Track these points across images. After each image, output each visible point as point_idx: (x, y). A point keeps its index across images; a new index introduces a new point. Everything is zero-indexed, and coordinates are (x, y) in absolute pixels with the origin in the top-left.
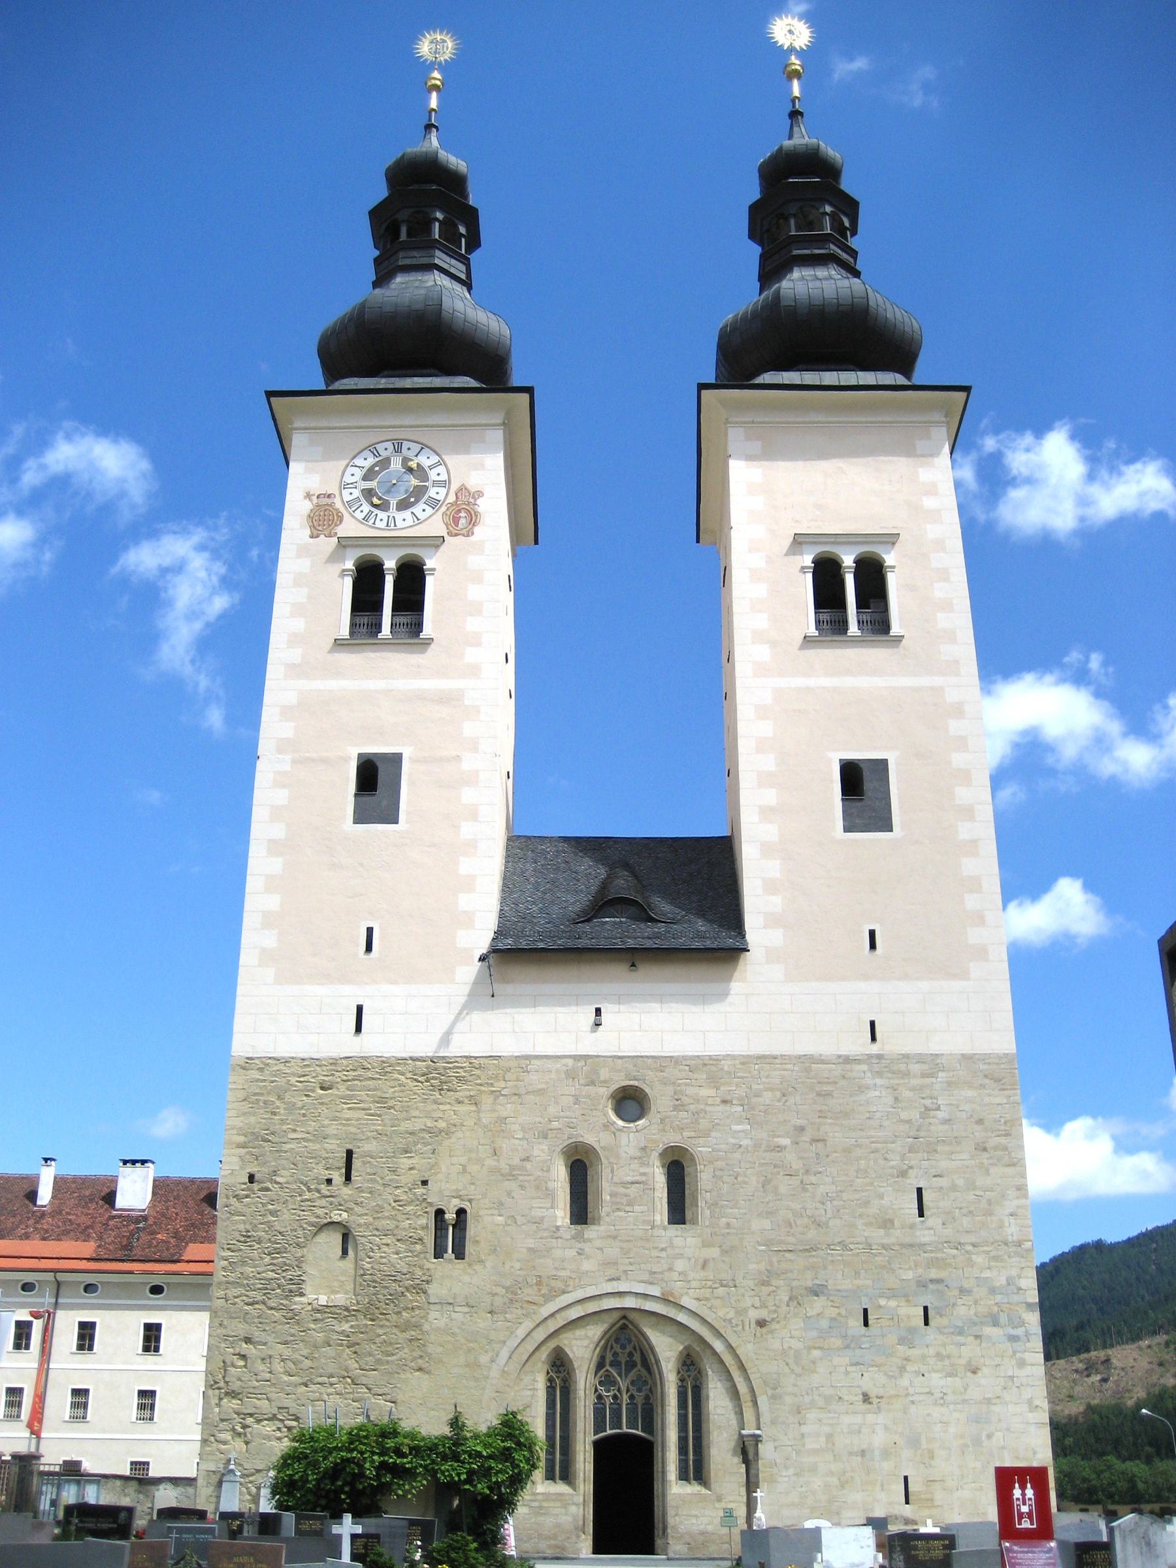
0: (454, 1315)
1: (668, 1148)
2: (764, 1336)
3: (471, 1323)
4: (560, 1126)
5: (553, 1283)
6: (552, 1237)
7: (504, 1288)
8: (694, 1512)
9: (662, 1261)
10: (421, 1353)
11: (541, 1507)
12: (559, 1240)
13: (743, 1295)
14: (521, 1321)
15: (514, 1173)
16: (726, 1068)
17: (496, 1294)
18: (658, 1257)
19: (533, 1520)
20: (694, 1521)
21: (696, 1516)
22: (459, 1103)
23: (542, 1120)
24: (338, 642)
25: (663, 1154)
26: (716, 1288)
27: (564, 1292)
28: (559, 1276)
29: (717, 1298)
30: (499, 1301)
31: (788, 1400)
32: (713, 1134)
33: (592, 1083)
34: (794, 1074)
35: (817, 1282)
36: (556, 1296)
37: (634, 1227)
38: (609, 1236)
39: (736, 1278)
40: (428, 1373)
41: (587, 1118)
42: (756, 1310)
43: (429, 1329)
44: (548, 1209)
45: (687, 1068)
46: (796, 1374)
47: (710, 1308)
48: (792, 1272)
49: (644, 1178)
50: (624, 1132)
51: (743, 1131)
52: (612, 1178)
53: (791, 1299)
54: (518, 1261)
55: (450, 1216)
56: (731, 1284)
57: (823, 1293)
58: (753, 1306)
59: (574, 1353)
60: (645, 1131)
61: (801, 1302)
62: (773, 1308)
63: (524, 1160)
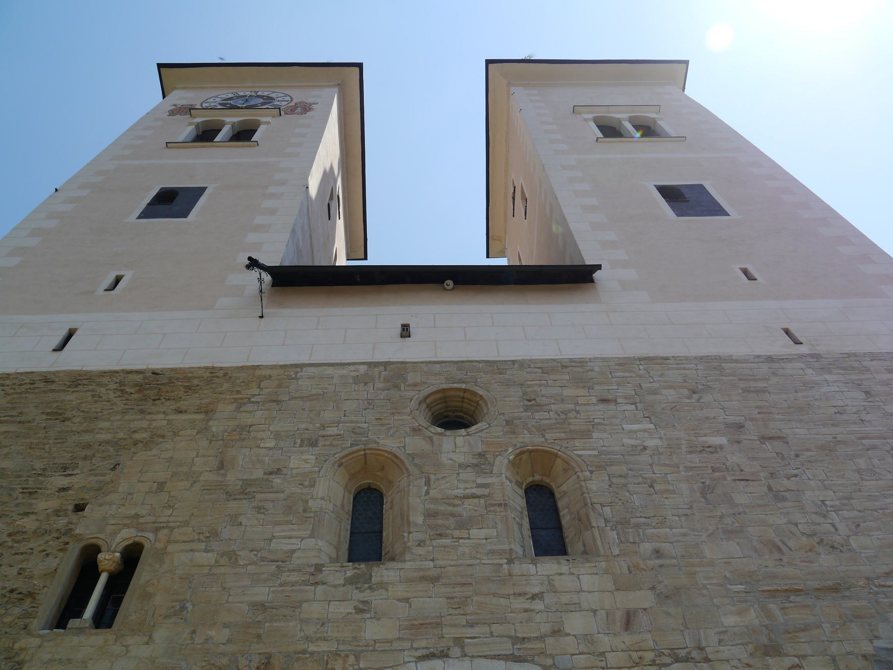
1: (522, 453)
4: (342, 432)
6: (305, 583)
9: (538, 618)
12: (320, 587)
15: (247, 491)
16: (597, 369)
18: (526, 611)
22: (181, 412)
23: (311, 426)
24: (168, 145)
25: (514, 464)
28: (312, 653)
32: (595, 435)
33: (397, 387)
34: (700, 372)
35: (878, 643)
37: (469, 562)
38: (423, 578)
39: (704, 644)
41: (386, 422)
44: (303, 539)
45: (540, 370)
49: (486, 491)
50: (446, 435)
51: (645, 431)
52: (427, 493)
54: (226, 626)
55: (109, 560)
56: (695, 654)
60: (483, 434)
63: (271, 473)
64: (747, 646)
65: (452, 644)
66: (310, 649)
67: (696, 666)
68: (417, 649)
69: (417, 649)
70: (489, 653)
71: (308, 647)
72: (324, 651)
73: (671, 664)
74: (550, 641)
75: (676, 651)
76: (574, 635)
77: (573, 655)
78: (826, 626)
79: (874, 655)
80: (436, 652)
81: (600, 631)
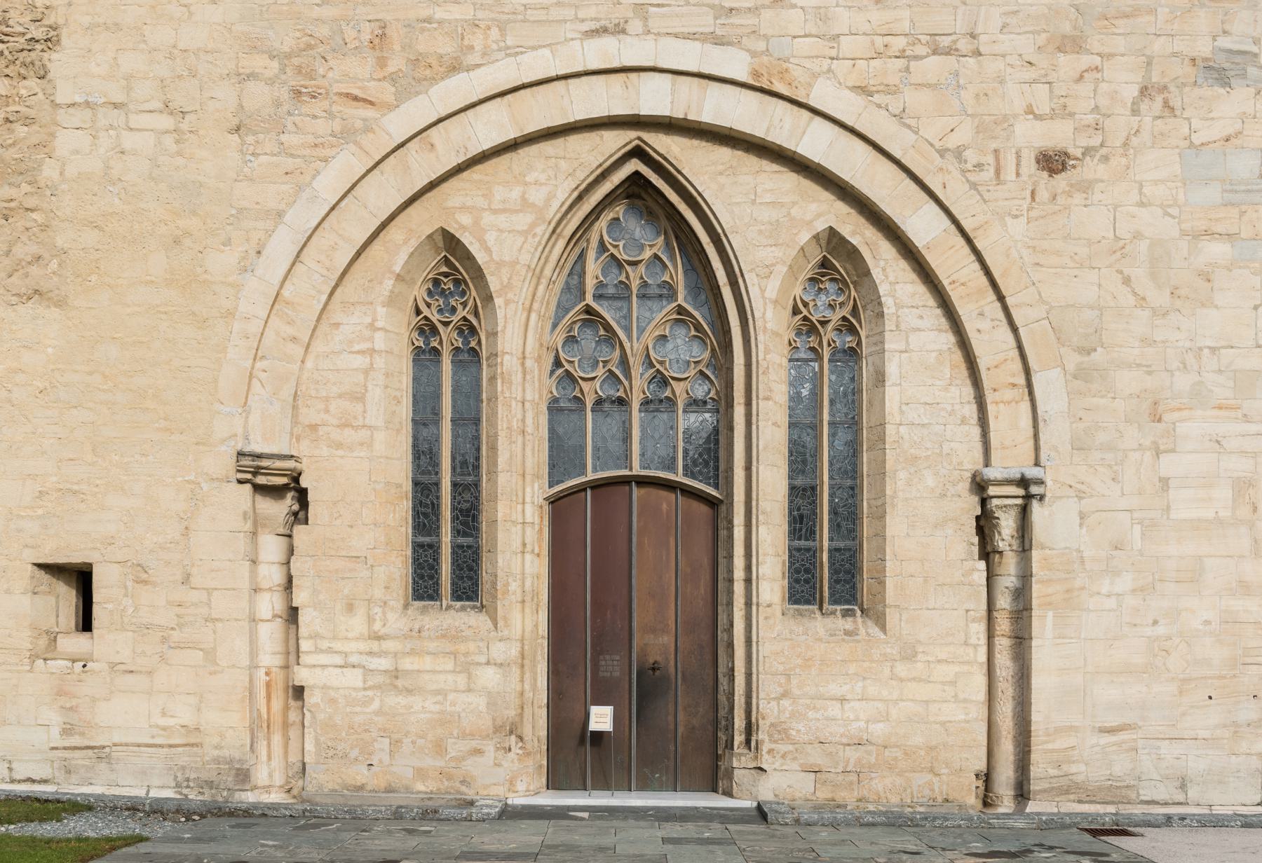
0: (129, 141)
2: (1061, 200)
3: (180, 161)
5: (423, 45)
7: (272, 57)
8: (834, 689)
10: (34, 249)
11: (396, 674)
13: (1002, 82)
14: (327, 152)
17: (252, 76)
19: (376, 705)
20: (834, 710)
21: (843, 700)
26: (917, 58)
27: (455, 68)
29: (919, 85)
30: (258, 96)
31: (1128, 381)
36: (433, 80)
39: (979, 30)
40: (61, 303)
42: (1038, 123)
43: (55, 175)
46: (1154, 311)
47: (899, 117)
48: (1152, 11)
53: (1144, 91)
56: (964, 45)
57: (1244, 76)
58: (1030, 111)
59: (488, 250)
61: (1176, 102)
62: (1090, 119)
64: (1039, 35)
65: (631, 15)
66: (437, 16)
67: (958, 61)
68: (583, 21)
69: (583, 21)
70: (682, 30)
71: (434, 13)
72: (456, 20)
73: (926, 57)
74: (767, 14)
75: (937, 38)
76: (802, 8)
77: (795, 37)
78: (1163, 12)
79: (1205, 60)
80: (610, 26)
81: (841, 2)
